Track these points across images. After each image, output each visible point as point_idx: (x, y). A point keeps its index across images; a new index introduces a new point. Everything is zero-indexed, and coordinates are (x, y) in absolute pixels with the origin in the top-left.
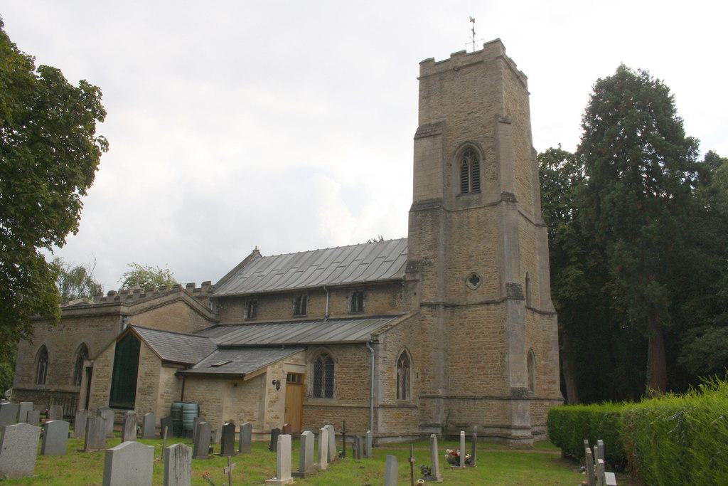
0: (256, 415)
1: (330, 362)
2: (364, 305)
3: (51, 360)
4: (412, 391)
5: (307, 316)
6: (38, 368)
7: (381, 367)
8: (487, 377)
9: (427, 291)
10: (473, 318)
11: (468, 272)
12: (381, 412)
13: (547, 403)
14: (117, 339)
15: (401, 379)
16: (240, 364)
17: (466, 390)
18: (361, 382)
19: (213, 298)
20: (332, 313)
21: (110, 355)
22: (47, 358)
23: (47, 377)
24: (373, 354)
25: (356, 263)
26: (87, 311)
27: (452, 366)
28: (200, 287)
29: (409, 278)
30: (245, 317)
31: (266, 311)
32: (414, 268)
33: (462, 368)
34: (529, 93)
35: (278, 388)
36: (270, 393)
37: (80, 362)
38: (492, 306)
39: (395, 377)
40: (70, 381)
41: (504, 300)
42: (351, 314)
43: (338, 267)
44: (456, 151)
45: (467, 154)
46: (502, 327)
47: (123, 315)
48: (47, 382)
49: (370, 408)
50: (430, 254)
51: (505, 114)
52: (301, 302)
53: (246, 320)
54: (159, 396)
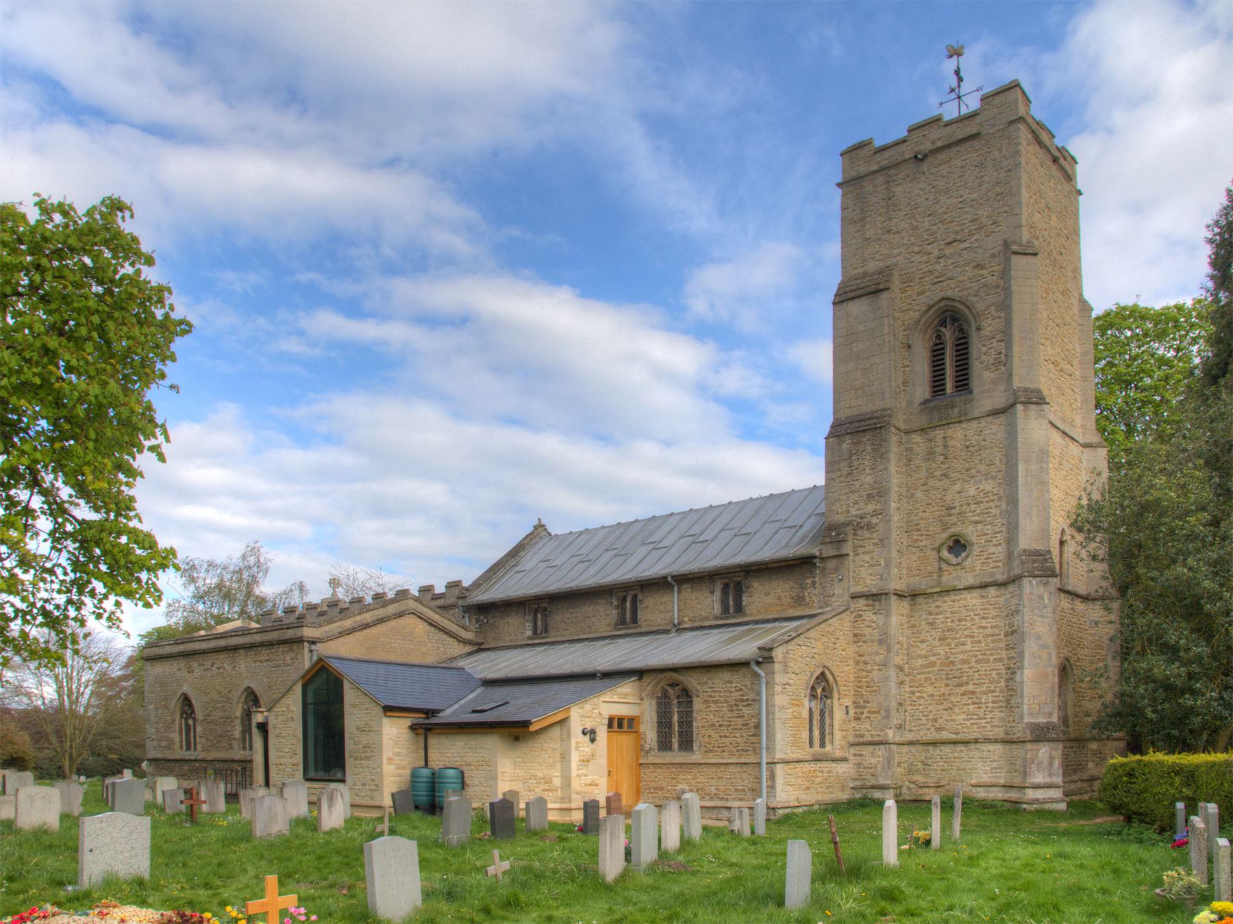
0: (557, 782)
1: (686, 695)
2: (744, 603)
3: (199, 715)
4: (838, 735)
5: (640, 626)
6: (181, 729)
7: (780, 700)
8: (980, 708)
9: (864, 572)
10: (951, 613)
11: (945, 535)
12: (780, 770)
13: (240, 886)
14: (303, 677)
15: (816, 717)
16: (518, 704)
17: (938, 730)
18: (744, 725)
19: (467, 606)
20: (686, 619)
21: (293, 704)
22: (193, 712)
23: (198, 739)
24: (764, 680)
25: (727, 534)
26: (246, 640)
27: (913, 693)
28: (443, 590)
29: (829, 551)
30: (529, 633)
31: (563, 620)
32: (838, 535)
33: (933, 695)
34: (1079, 193)
35: (593, 740)
36: (579, 746)
37: (248, 715)
38: (992, 591)
39: (805, 714)
40: (236, 745)
41: (1015, 580)
42: (721, 619)
43: (654, 549)
44: (971, 311)
45: (943, 323)
46: (1011, 625)
47: (309, 642)
48: (199, 747)
49: (759, 764)
50: (870, 507)
51: (1025, 236)
52: (628, 604)
53: (529, 638)
54: (385, 761)
